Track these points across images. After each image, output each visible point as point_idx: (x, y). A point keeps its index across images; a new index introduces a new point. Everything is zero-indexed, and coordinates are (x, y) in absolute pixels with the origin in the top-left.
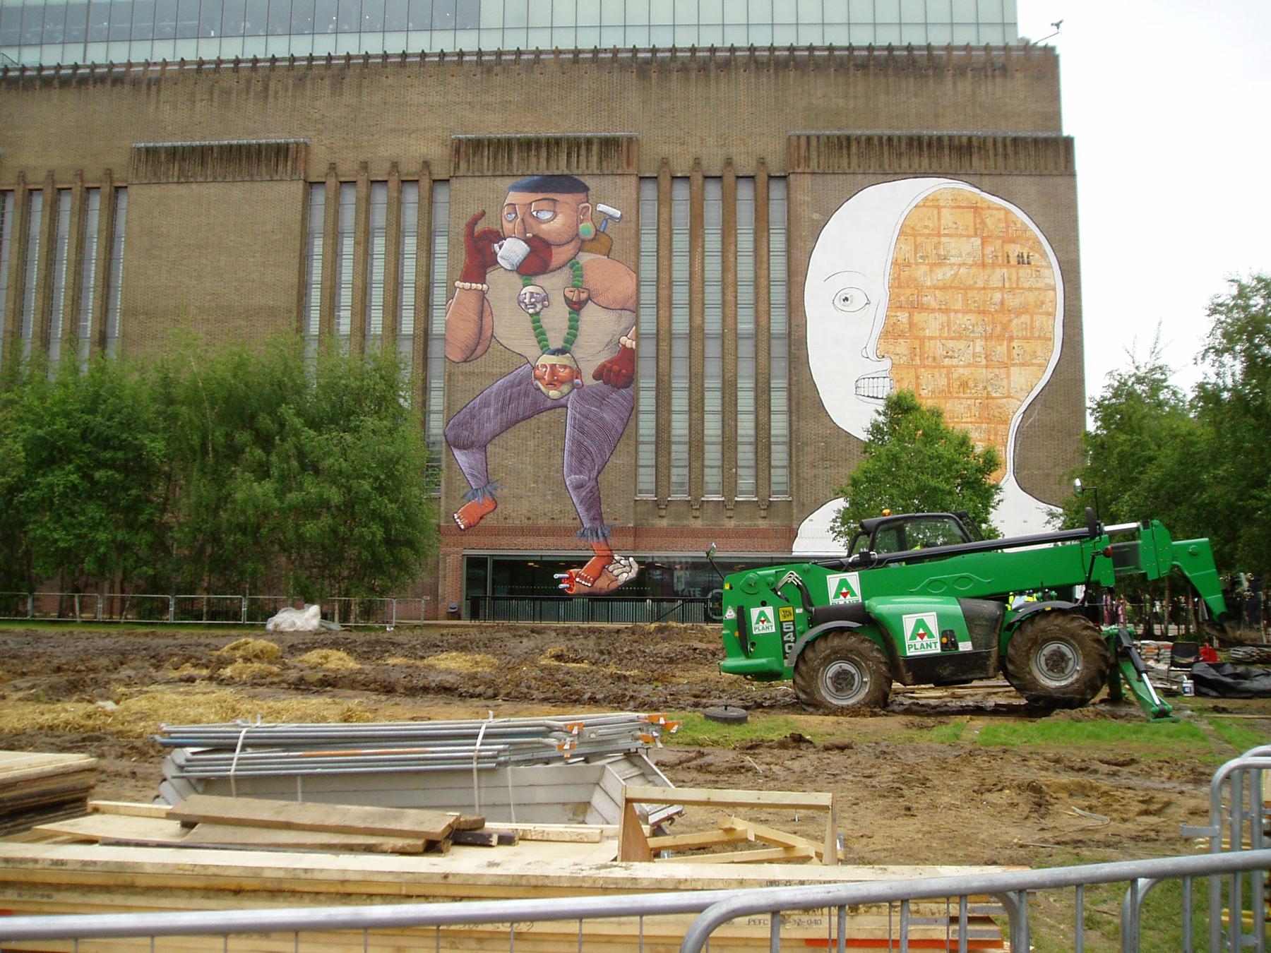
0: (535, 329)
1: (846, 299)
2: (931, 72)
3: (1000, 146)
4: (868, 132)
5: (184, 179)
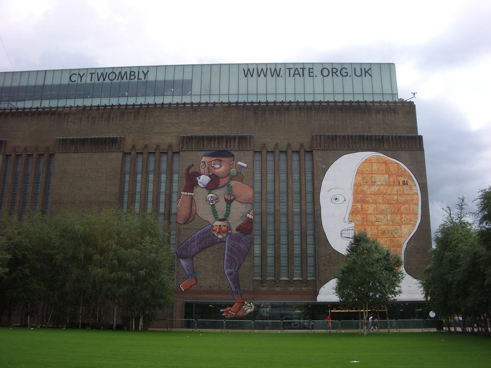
0: (213, 211)
1: (336, 199)
2: (367, 111)
3: (394, 139)
4: (343, 134)
5: (76, 152)
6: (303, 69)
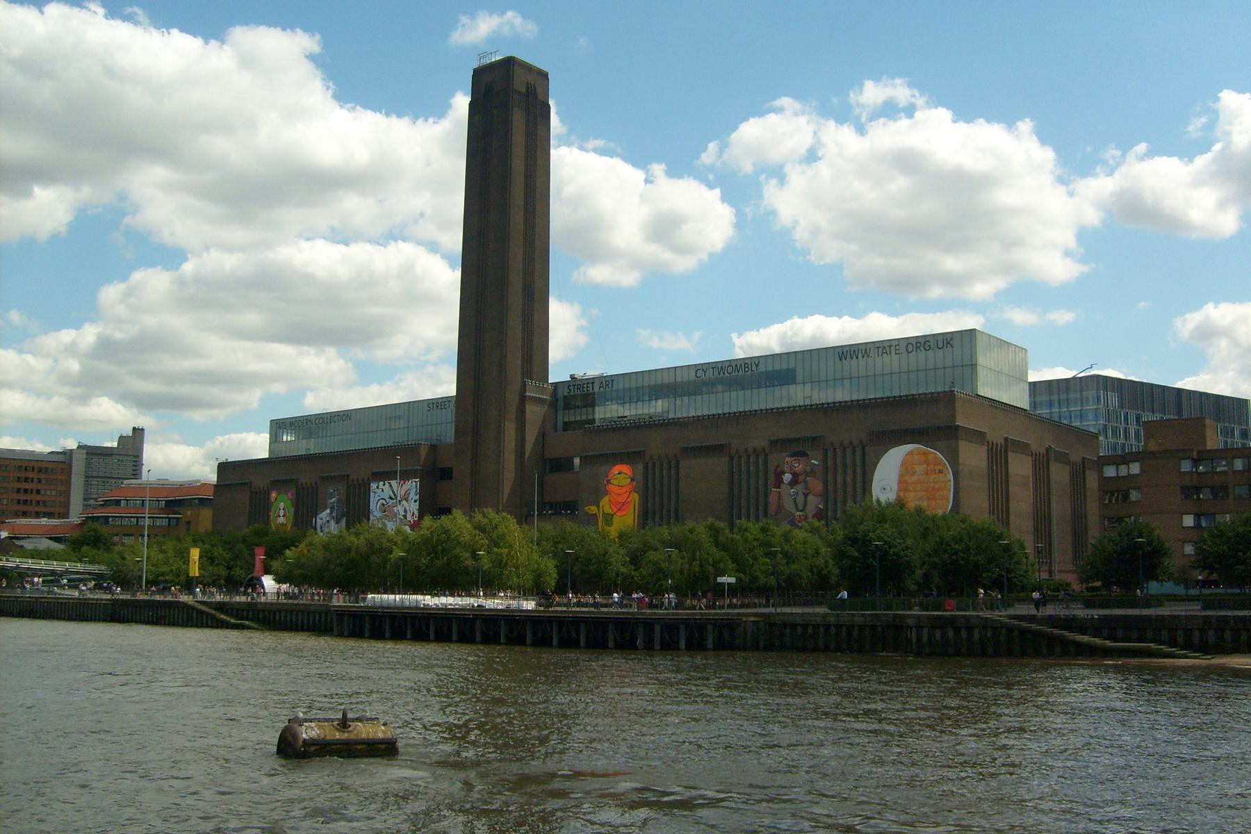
6: (890, 346)
